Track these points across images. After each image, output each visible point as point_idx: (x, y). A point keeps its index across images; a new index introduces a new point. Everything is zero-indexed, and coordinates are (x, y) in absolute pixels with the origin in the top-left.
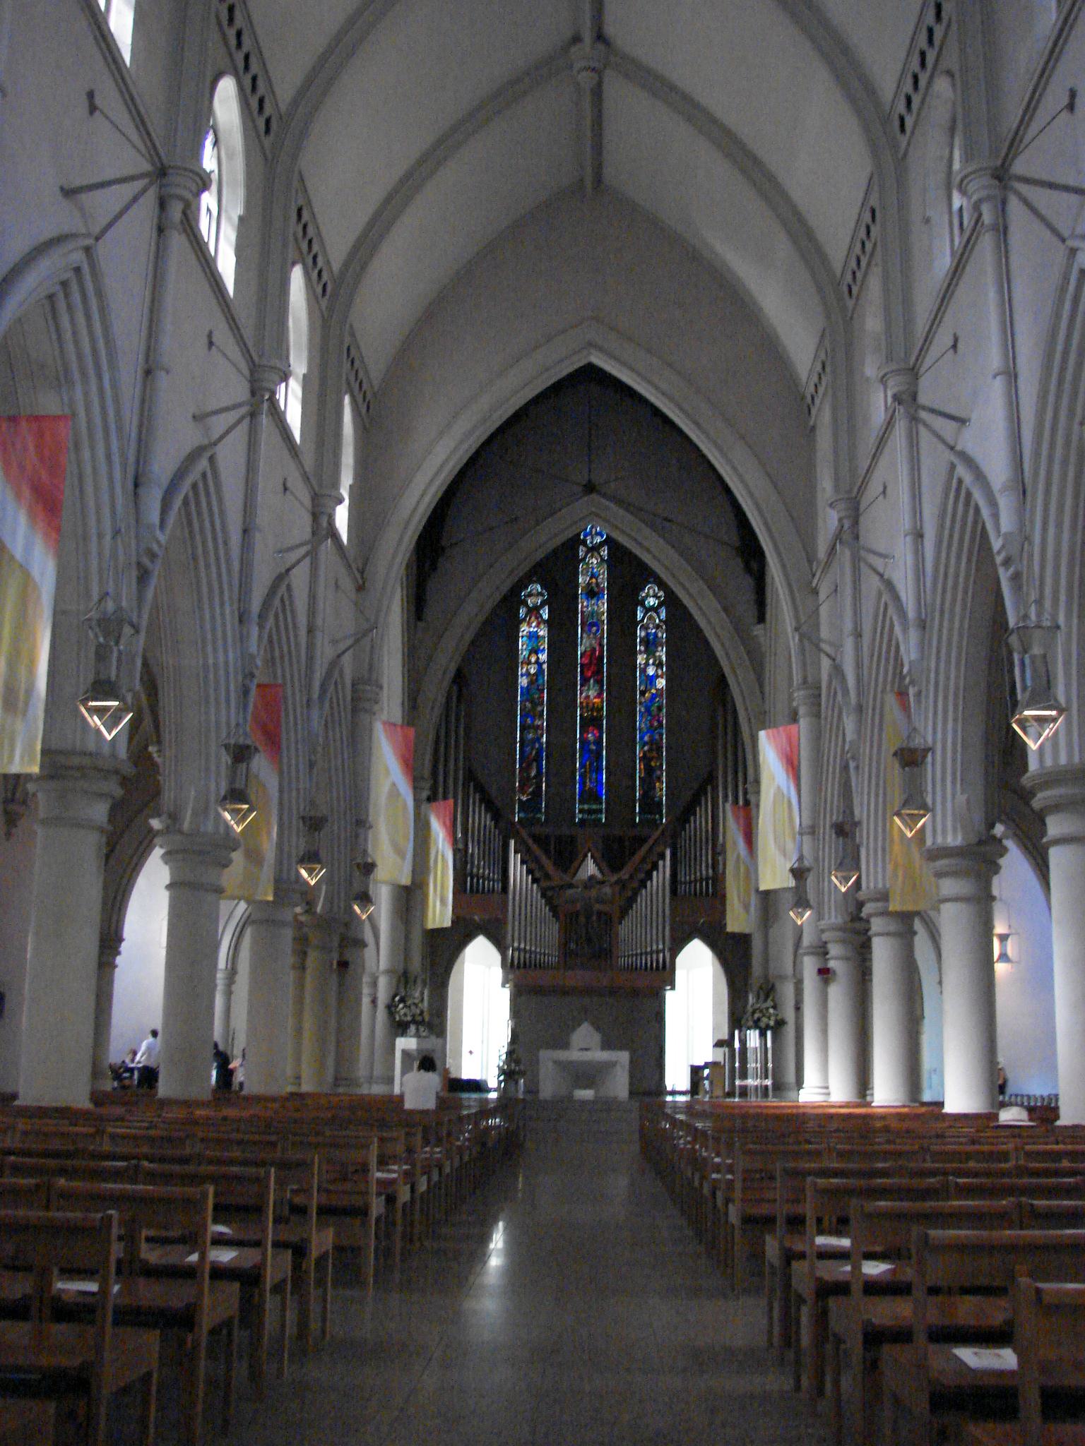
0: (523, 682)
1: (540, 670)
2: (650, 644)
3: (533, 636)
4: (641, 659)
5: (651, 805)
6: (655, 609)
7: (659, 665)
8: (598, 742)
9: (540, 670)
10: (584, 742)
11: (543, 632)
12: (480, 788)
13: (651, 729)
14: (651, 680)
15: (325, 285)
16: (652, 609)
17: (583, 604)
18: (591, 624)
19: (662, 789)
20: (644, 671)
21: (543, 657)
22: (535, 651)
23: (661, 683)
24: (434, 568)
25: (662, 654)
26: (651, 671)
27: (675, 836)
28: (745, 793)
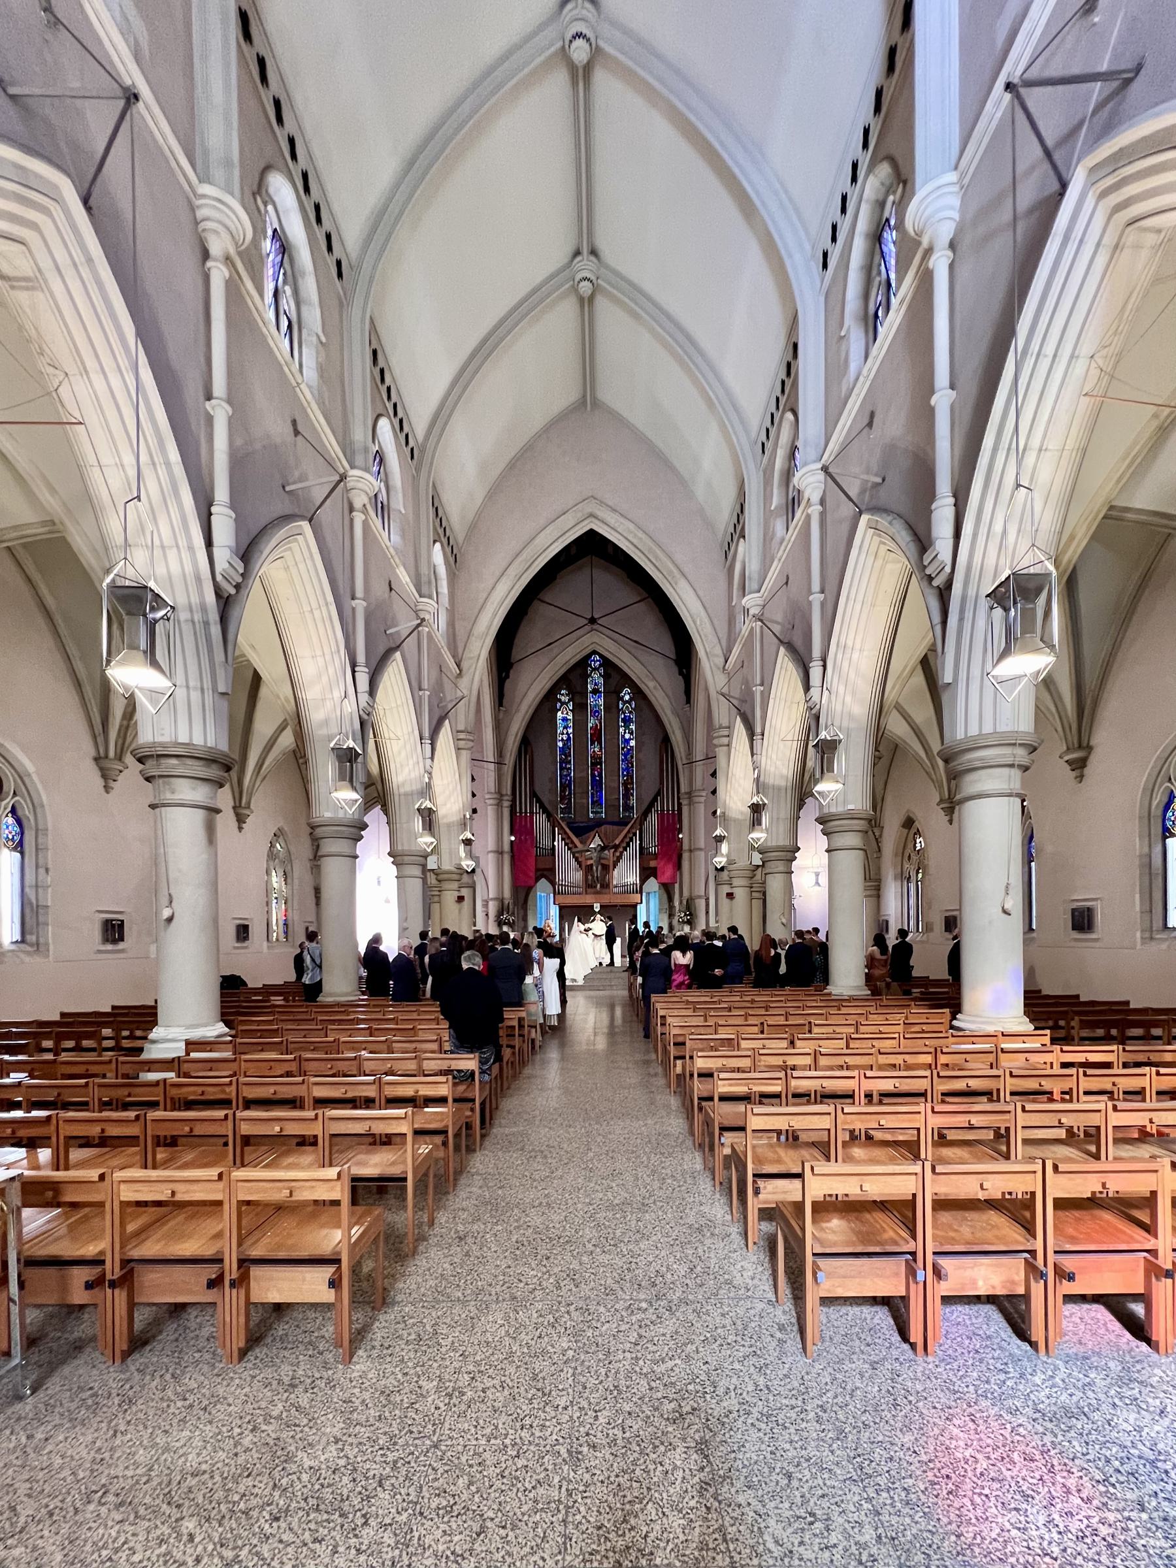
0: (560, 744)
1: (569, 738)
2: (627, 721)
3: (565, 719)
4: (621, 730)
5: (628, 808)
6: (629, 702)
7: (631, 733)
8: (600, 775)
9: (569, 738)
10: (593, 775)
11: (570, 717)
12: (539, 801)
13: (627, 769)
14: (627, 741)
15: (412, 449)
16: (627, 702)
17: (591, 700)
18: (595, 713)
19: (633, 801)
20: (623, 736)
21: (570, 731)
22: (566, 727)
23: (633, 743)
24: (507, 676)
25: (633, 727)
26: (627, 736)
27: (641, 824)
28: (679, 798)
